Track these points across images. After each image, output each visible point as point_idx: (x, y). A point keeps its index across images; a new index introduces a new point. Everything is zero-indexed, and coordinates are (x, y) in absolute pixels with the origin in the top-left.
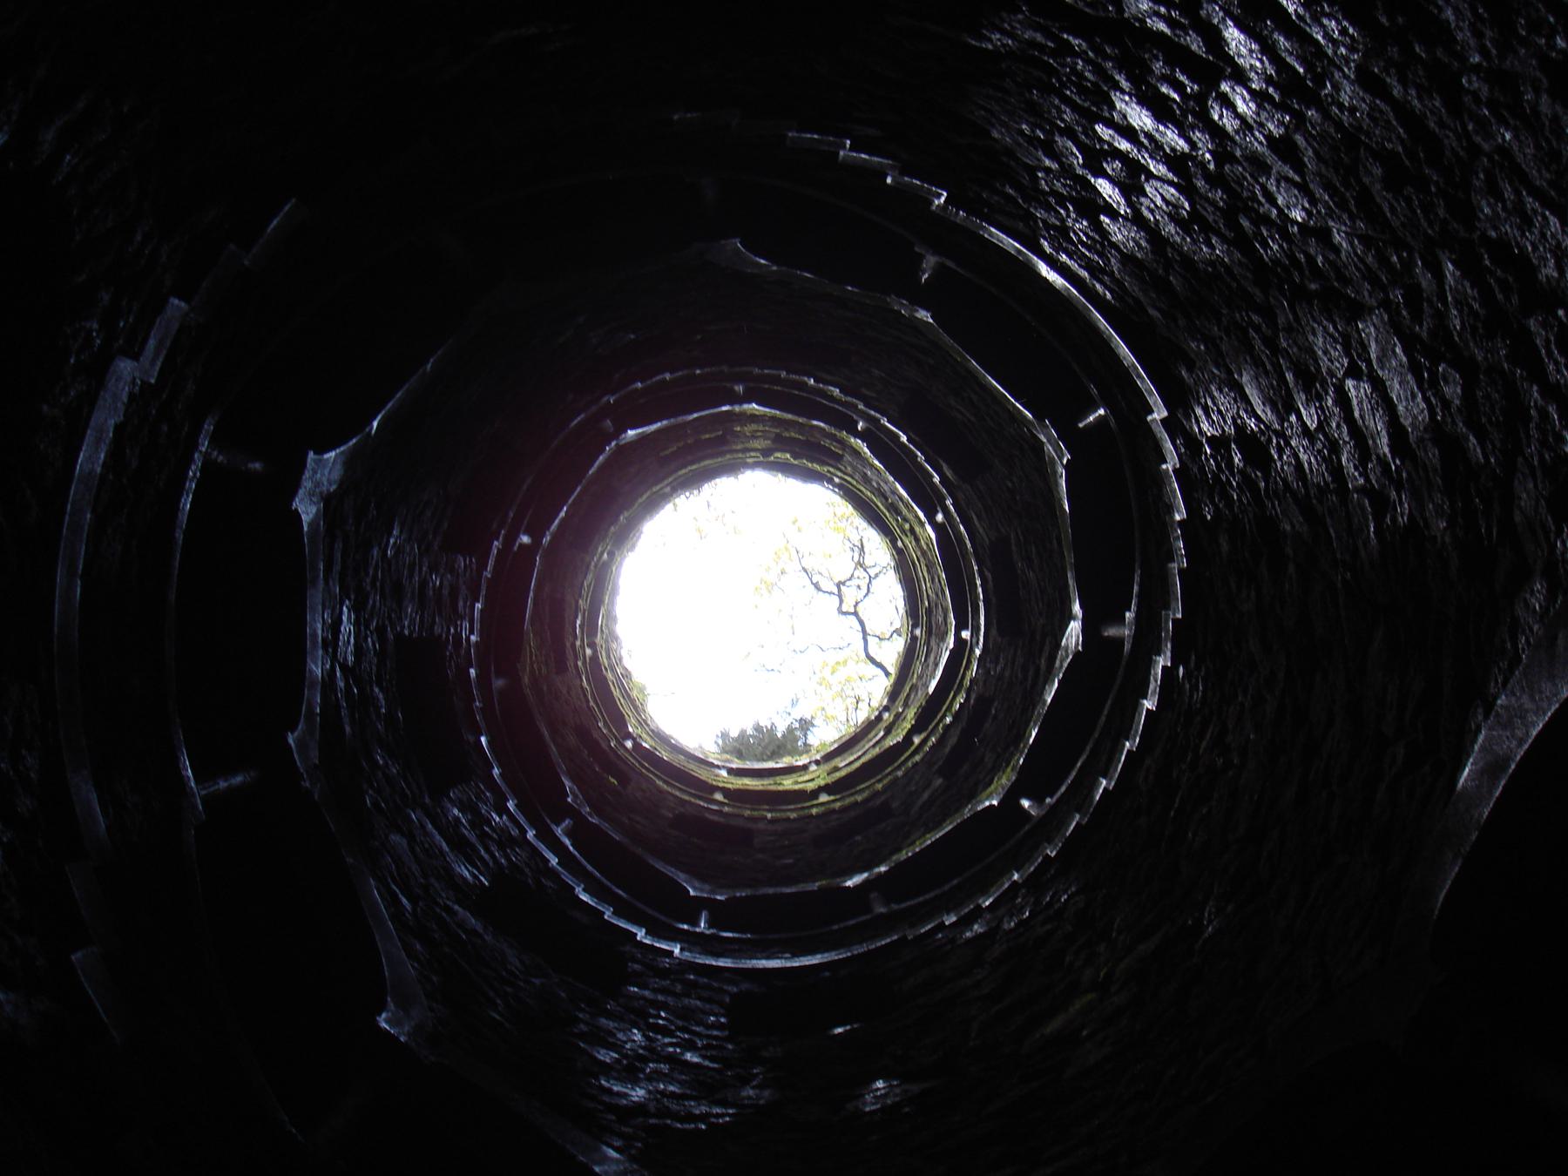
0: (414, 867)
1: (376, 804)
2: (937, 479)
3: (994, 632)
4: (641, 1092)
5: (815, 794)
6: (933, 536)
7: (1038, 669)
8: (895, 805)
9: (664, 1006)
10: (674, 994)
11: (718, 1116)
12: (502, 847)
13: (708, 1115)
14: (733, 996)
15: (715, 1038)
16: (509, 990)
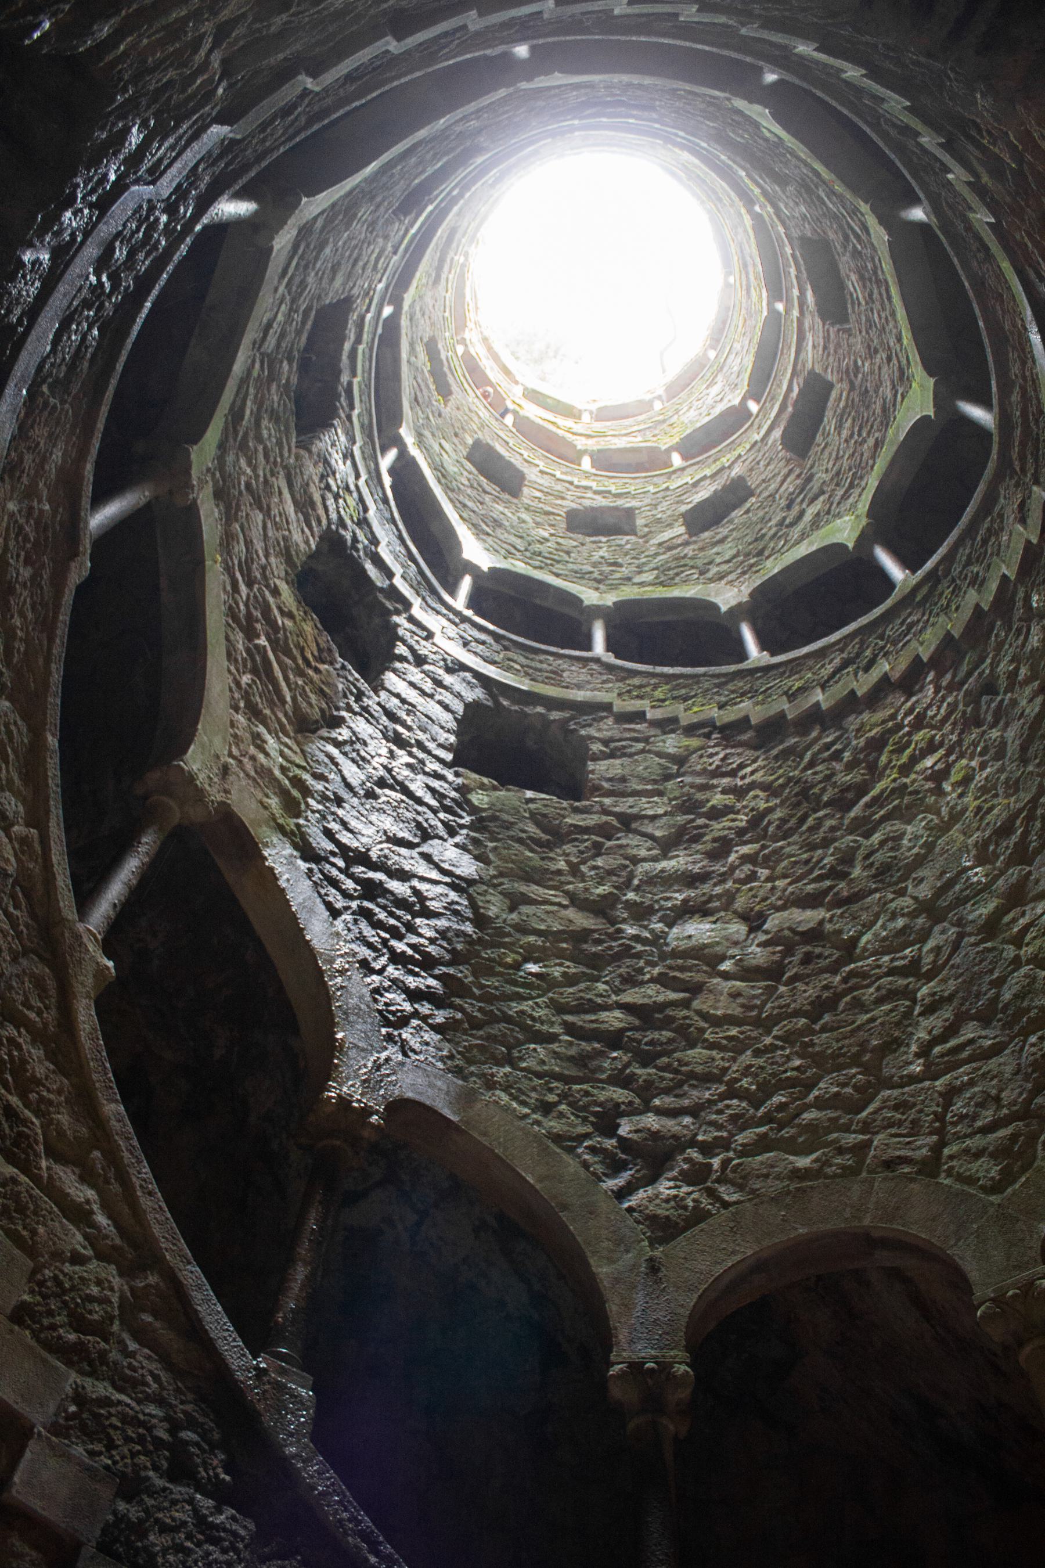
0: (259, 546)
1: (248, 485)
2: (796, 292)
3: (777, 433)
4: (370, 831)
5: (582, 453)
6: (765, 313)
7: (802, 514)
8: (640, 522)
9: (411, 709)
10: (423, 693)
11: (422, 879)
12: (337, 497)
13: (414, 876)
14: (467, 706)
15: (441, 761)
16: (300, 683)
